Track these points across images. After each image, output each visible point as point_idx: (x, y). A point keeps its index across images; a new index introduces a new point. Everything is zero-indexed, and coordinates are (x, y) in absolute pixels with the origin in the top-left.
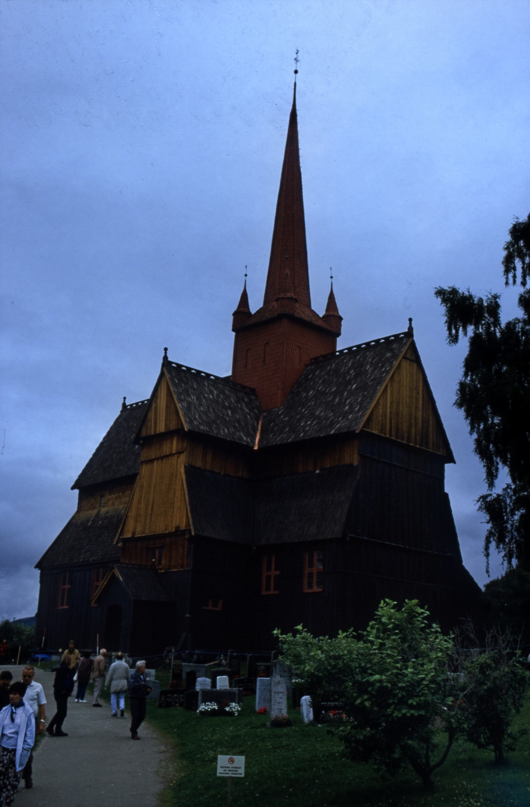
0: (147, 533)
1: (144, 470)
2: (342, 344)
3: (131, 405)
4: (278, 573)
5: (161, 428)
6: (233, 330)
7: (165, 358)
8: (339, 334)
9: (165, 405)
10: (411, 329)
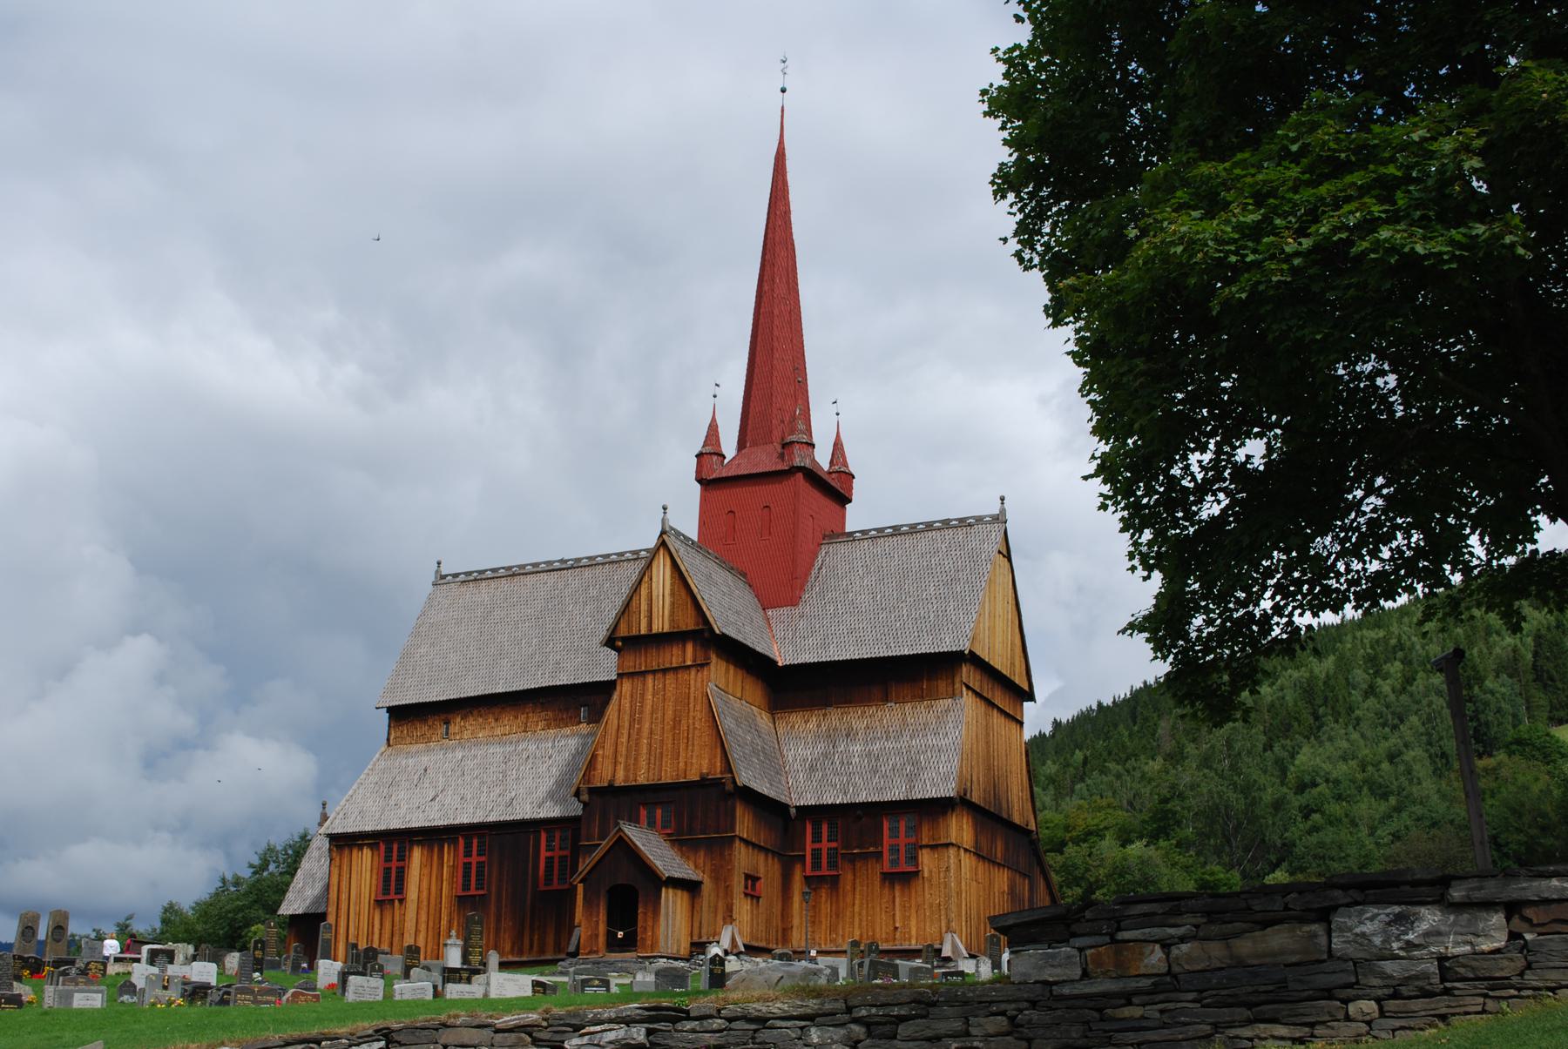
0: (642, 780)
1: (626, 687)
2: (856, 517)
3: (456, 575)
4: (834, 845)
5: (661, 625)
6: (699, 480)
7: (663, 521)
8: (850, 501)
9: (667, 591)
10: (1003, 511)
